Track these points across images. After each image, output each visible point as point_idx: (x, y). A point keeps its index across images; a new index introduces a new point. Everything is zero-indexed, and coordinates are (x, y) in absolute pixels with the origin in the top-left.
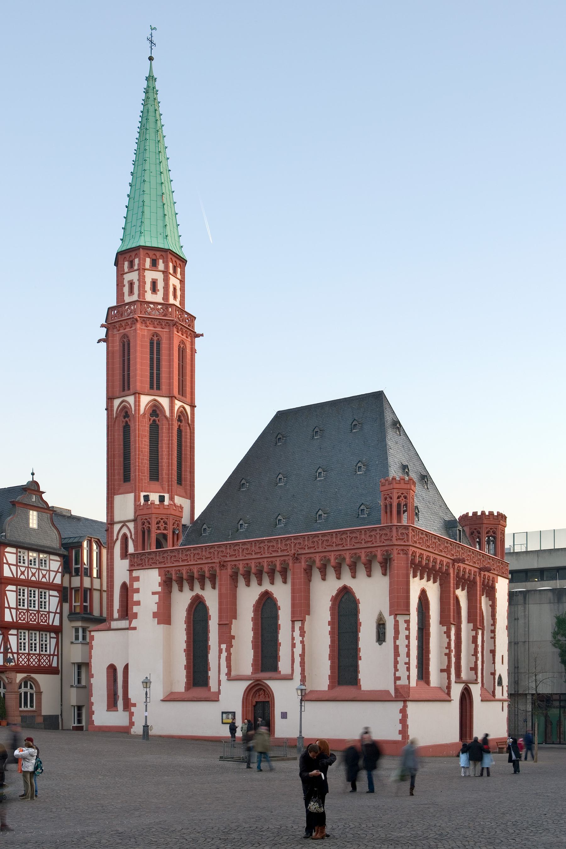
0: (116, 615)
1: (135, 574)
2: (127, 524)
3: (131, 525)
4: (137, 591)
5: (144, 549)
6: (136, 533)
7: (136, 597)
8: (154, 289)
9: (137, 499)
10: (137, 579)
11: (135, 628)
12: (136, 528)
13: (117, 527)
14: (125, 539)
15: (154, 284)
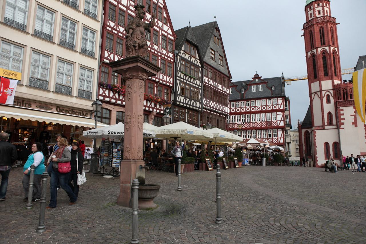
0: (326, 124)
1: (341, 108)
2: (330, 91)
3: (332, 92)
4: (343, 114)
5: (344, 99)
6: (334, 94)
7: (342, 117)
8: (327, 13)
9: (333, 82)
10: (342, 110)
11: (343, 128)
12: (333, 92)
13: (323, 93)
14: (328, 96)
15: (327, 11)
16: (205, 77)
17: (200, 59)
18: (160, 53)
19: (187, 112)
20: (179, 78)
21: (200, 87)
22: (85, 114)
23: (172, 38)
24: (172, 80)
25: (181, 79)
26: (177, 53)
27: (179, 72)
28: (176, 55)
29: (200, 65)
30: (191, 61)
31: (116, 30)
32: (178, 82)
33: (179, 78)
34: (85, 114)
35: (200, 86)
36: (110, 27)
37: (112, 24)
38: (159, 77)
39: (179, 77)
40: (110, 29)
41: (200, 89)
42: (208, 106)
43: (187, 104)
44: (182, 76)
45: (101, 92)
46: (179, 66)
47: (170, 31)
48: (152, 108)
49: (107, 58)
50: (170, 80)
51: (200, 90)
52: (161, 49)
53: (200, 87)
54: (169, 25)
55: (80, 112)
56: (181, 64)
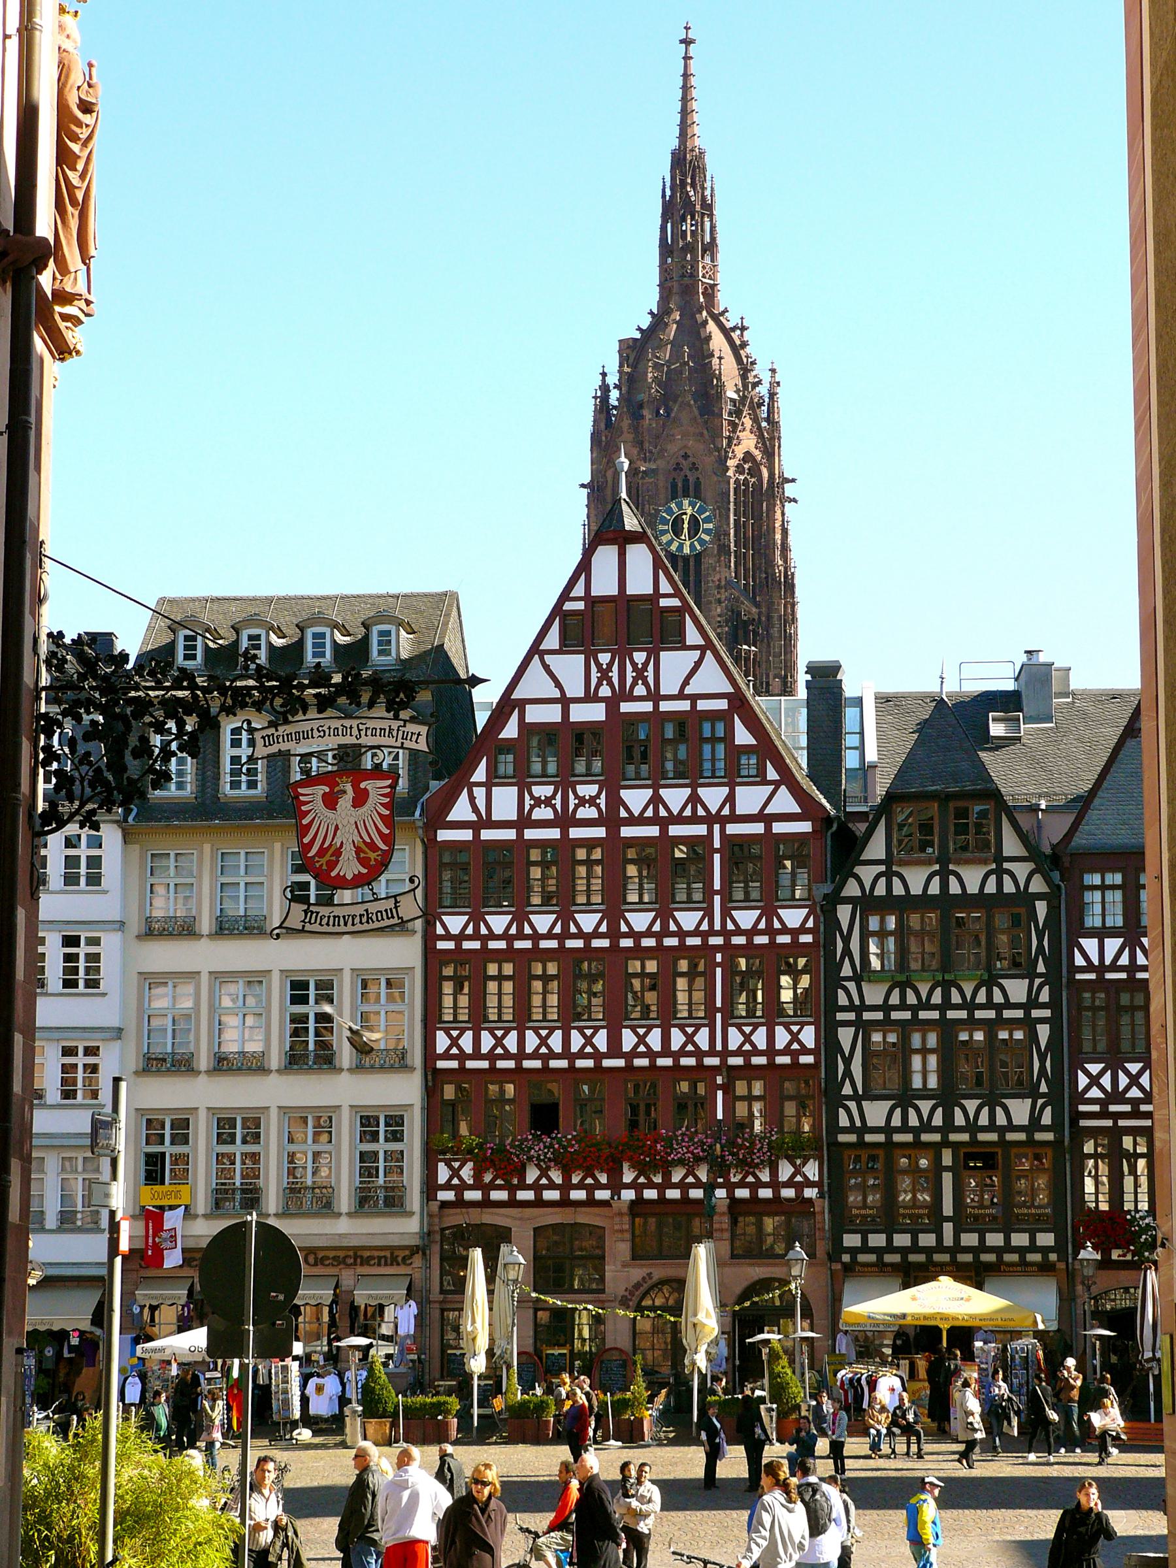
16: (1090, 945)
17: (1033, 854)
18: (724, 932)
19: (947, 1158)
20: (851, 1016)
21: (1036, 1013)
22: (400, 1259)
23: (805, 827)
24: (808, 1036)
25: (867, 1016)
26: (826, 896)
27: (851, 986)
28: (825, 909)
29: (1038, 885)
30: (954, 888)
31: (476, 936)
32: (845, 1036)
33: (851, 1016)
34: (400, 1259)
35: (1043, 1006)
36: (448, 936)
37: (455, 923)
38: (719, 1047)
39: (851, 1008)
40: (450, 945)
41: (1042, 1021)
42: (1135, 1102)
43: (926, 1127)
44: (874, 994)
45: (443, 1174)
46: (847, 952)
47: (785, 802)
48: (698, 1184)
49: (446, 1056)
50: (795, 1037)
51: (1044, 1032)
52: (726, 913)
53: (1047, 1013)
54: (772, 774)
55: (382, 1254)
56: (865, 935)
